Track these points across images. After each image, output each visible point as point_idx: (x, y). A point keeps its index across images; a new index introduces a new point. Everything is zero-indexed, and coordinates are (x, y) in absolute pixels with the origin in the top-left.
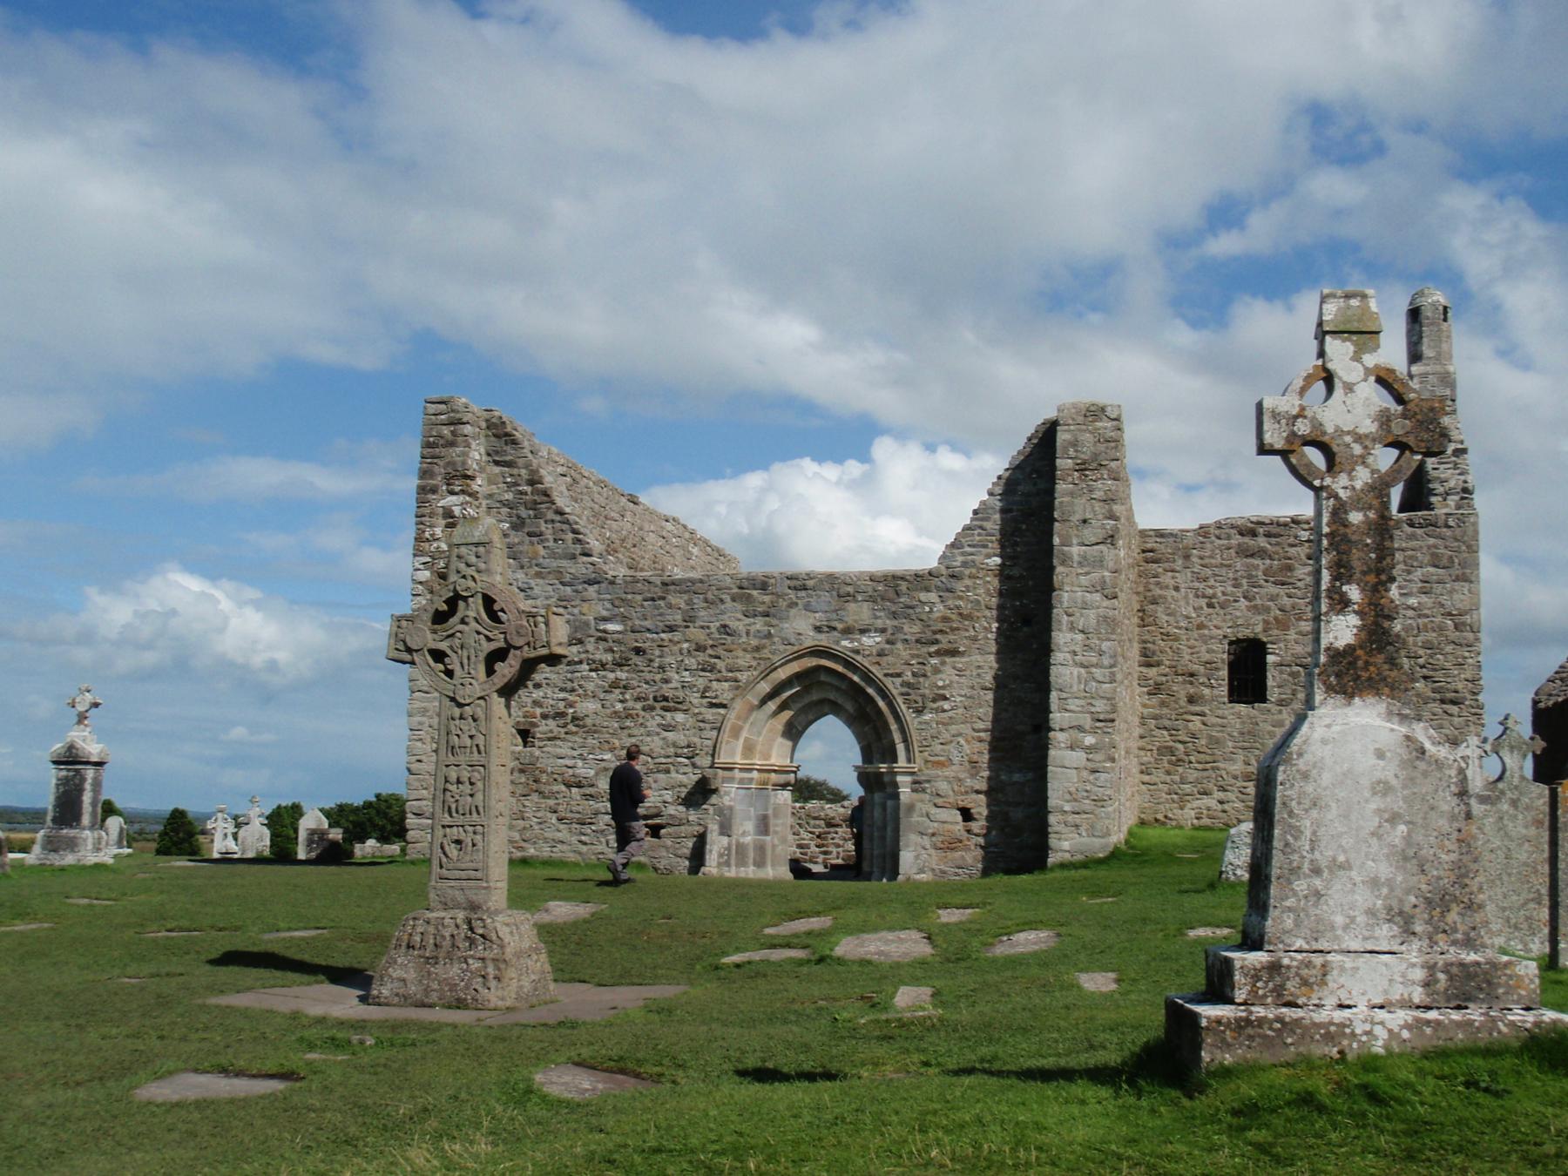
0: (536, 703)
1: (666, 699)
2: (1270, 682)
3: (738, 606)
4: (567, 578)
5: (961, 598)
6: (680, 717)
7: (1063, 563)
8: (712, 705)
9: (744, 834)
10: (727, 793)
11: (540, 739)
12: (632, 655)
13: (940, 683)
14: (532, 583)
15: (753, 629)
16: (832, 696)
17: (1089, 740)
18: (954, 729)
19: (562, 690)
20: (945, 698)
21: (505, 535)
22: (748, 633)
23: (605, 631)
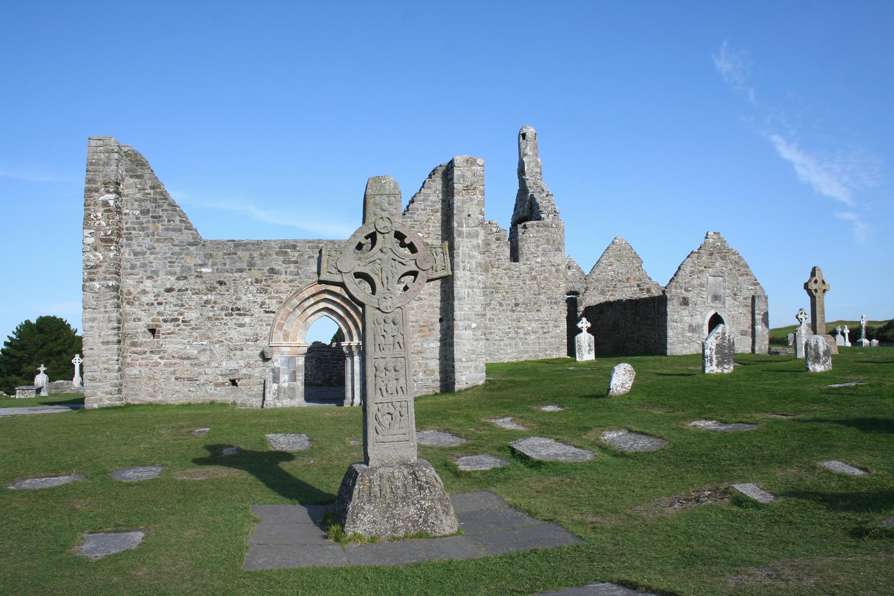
0: (159, 313)
1: (239, 310)
3: (281, 258)
4: (176, 242)
6: (247, 320)
8: (267, 312)
9: (284, 382)
10: (276, 360)
11: (163, 334)
12: (218, 285)
14: (156, 245)
15: (288, 270)
17: (474, 325)
19: (175, 305)
21: (137, 218)
22: (286, 272)
23: (200, 272)
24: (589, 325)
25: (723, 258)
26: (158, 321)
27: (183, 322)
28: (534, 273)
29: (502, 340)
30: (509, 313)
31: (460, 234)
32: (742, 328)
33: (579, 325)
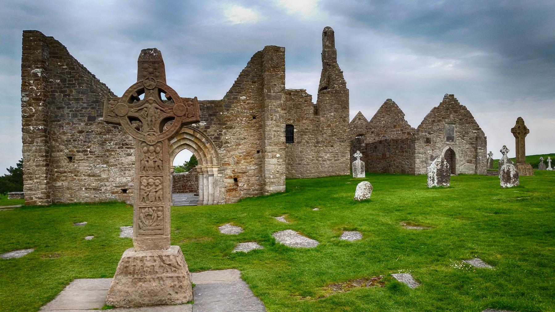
1: (127, 145)
2: (295, 137)
5: (233, 110)
7: (268, 98)
11: (77, 160)
13: (227, 138)
16: (188, 142)
17: (278, 155)
18: (232, 153)
20: (229, 143)
24: (361, 155)
25: (456, 112)
26: (73, 151)
27: (90, 152)
28: (329, 123)
29: (308, 165)
30: (313, 148)
31: (269, 97)
32: (468, 158)
33: (355, 155)
